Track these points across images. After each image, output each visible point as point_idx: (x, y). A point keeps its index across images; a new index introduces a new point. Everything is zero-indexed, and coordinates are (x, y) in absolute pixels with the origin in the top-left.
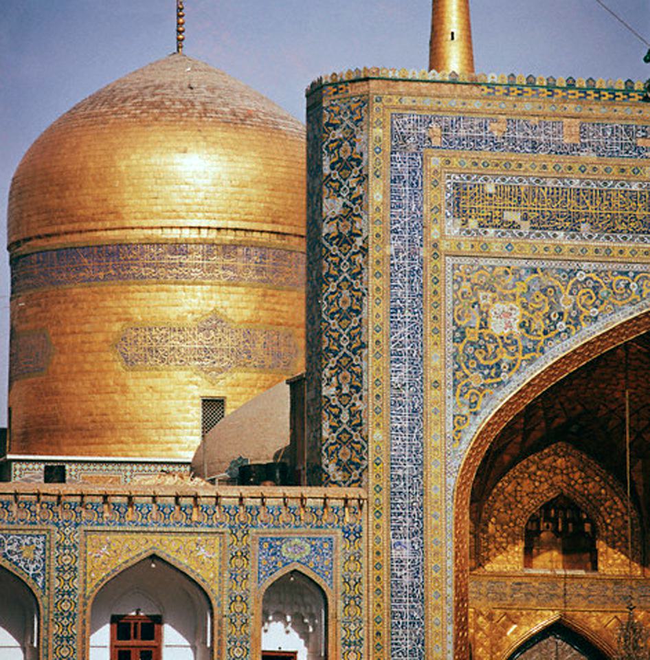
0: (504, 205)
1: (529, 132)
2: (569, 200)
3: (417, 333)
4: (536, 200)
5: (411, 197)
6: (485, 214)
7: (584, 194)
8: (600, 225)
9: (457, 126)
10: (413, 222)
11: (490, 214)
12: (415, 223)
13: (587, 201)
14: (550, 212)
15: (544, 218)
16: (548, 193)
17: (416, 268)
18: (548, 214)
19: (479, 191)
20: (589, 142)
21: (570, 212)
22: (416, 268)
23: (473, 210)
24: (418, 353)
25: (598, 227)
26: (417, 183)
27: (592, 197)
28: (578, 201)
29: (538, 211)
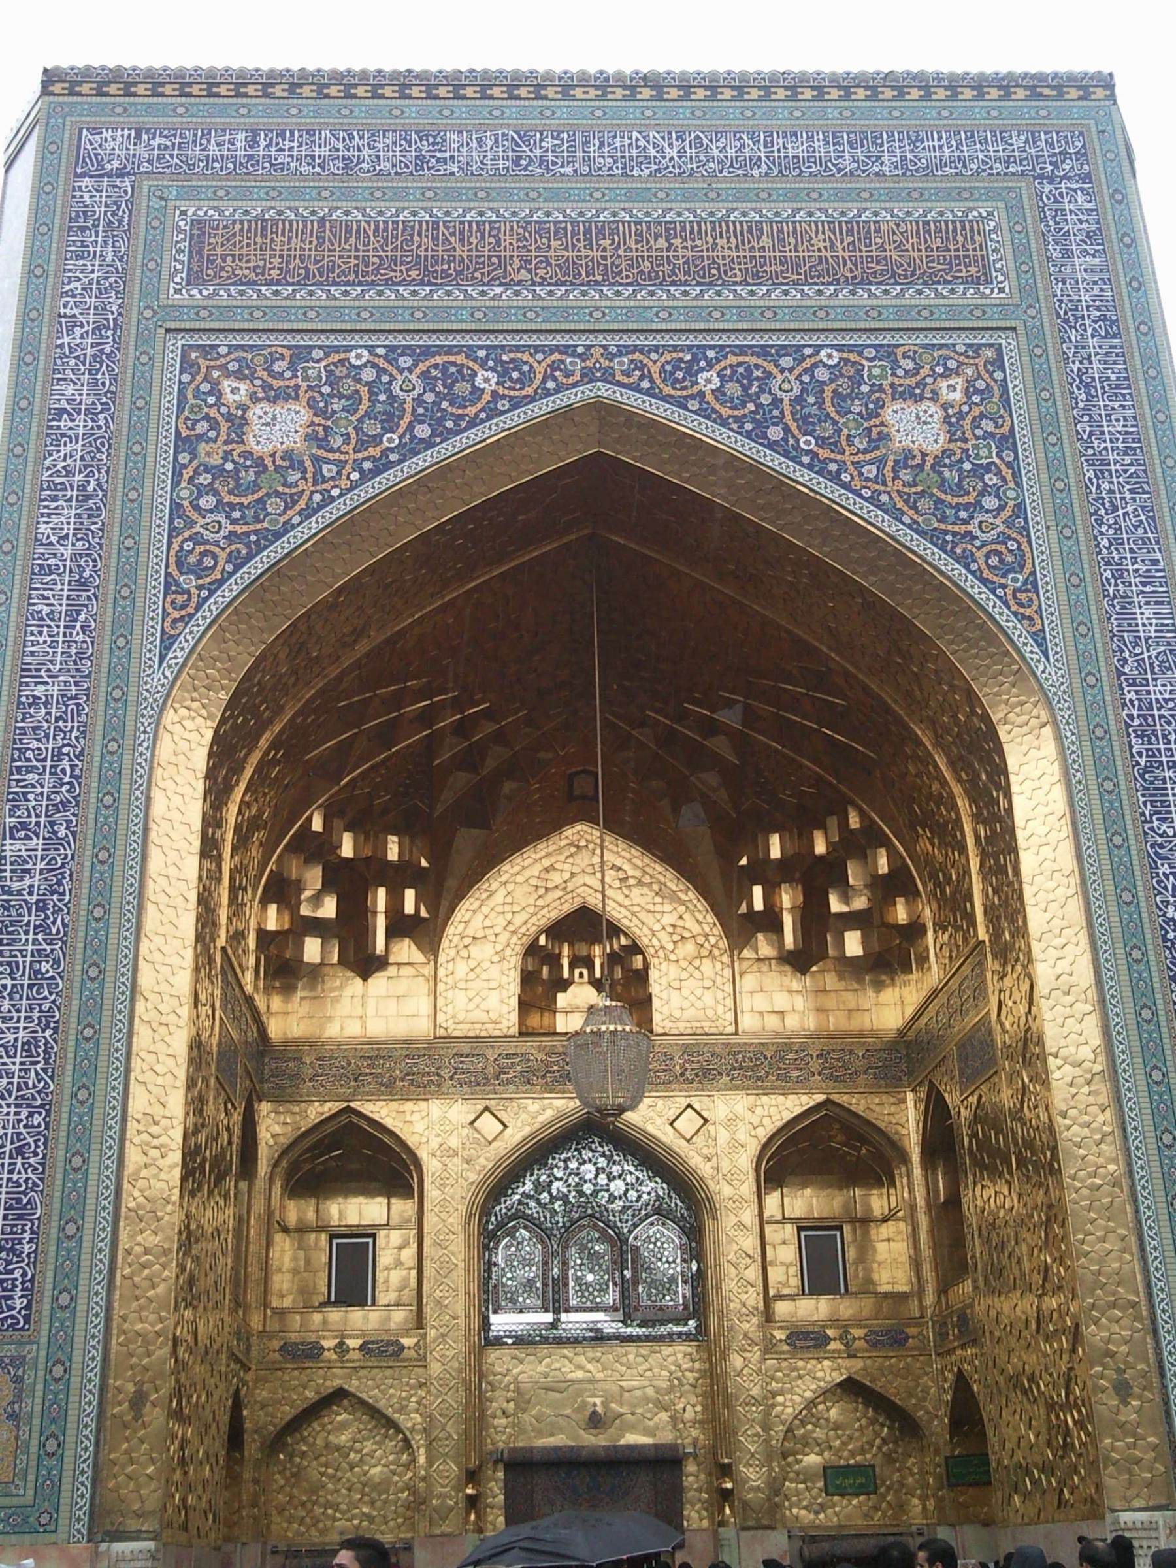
0: (289, 249)
1: (341, 146)
2: (416, 238)
3: (99, 451)
4: (352, 241)
5: (106, 243)
6: (251, 265)
7: (448, 228)
8: (477, 274)
9: (204, 141)
10: (106, 278)
11: (261, 263)
12: (112, 280)
13: (452, 240)
14: (380, 257)
15: (367, 266)
16: (376, 230)
17: (108, 350)
18: (376, 260)
19: (242, 230)
20: (452, 157)
21: (418, 256)
22: (108, 350)
23: (229, 259)
24: (99, 485)
25: (473, 278)
26: (120, 221)
27: (462, 232)
28: (435, 239)
29: (357, 257)
